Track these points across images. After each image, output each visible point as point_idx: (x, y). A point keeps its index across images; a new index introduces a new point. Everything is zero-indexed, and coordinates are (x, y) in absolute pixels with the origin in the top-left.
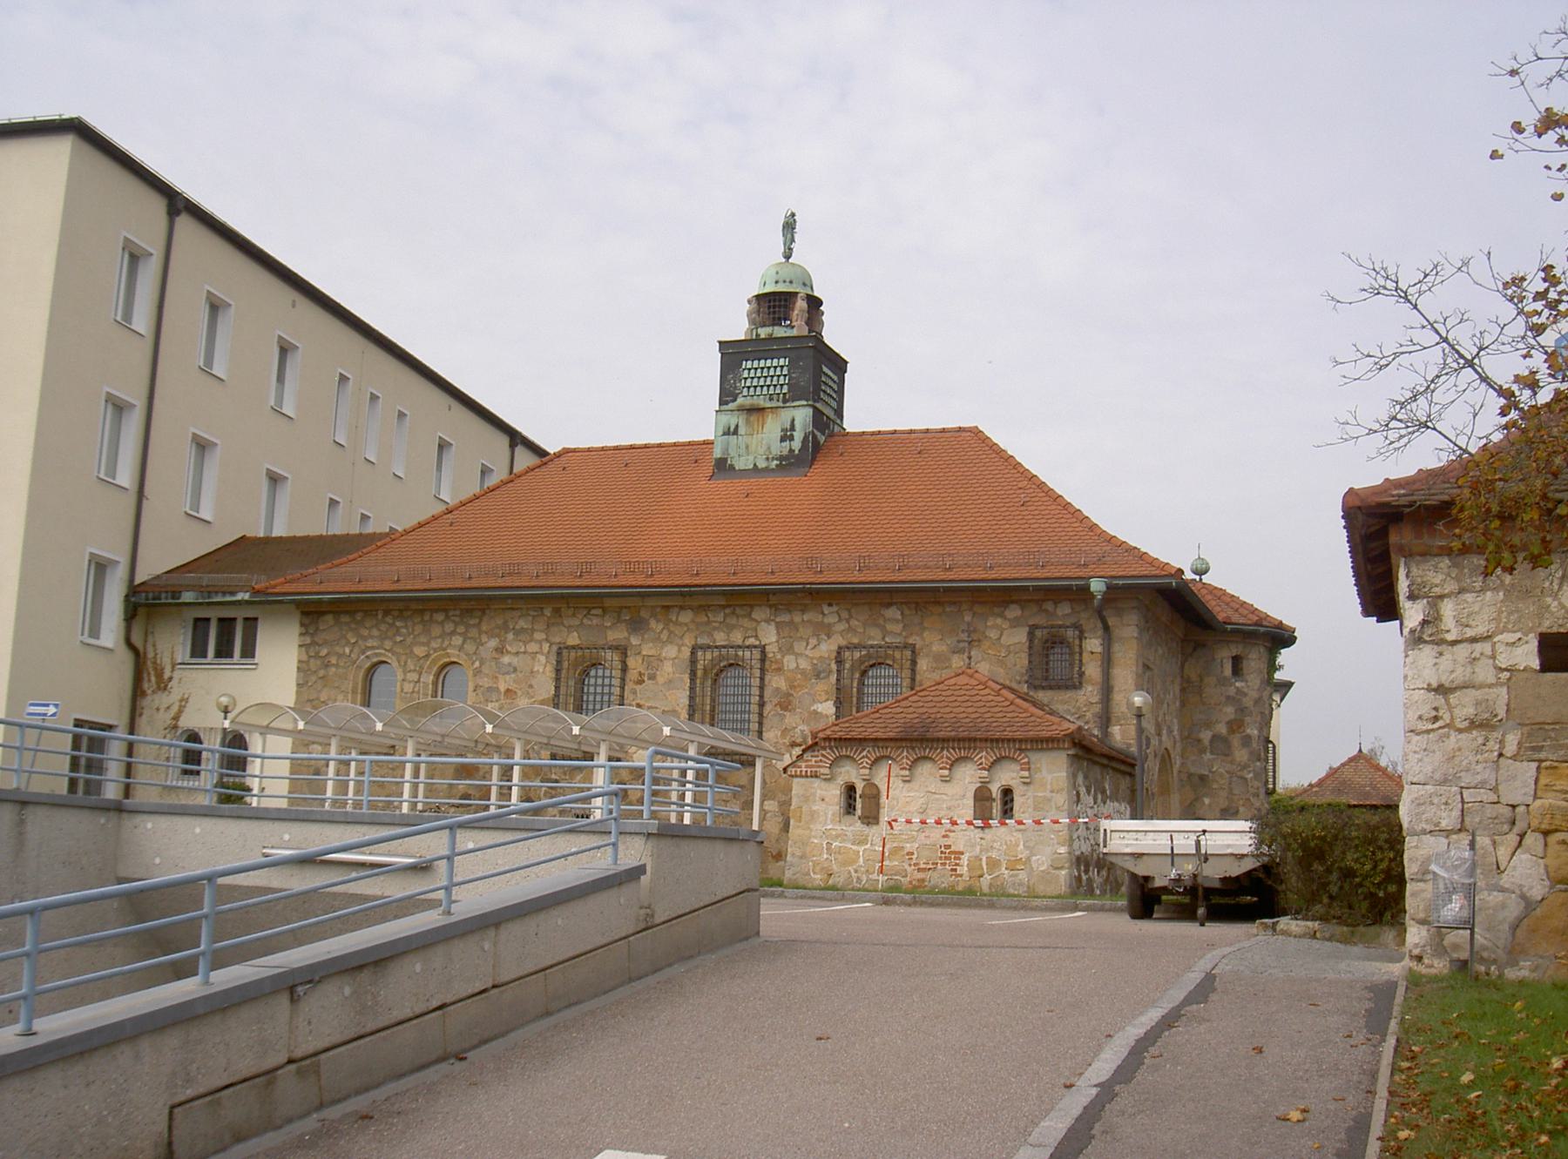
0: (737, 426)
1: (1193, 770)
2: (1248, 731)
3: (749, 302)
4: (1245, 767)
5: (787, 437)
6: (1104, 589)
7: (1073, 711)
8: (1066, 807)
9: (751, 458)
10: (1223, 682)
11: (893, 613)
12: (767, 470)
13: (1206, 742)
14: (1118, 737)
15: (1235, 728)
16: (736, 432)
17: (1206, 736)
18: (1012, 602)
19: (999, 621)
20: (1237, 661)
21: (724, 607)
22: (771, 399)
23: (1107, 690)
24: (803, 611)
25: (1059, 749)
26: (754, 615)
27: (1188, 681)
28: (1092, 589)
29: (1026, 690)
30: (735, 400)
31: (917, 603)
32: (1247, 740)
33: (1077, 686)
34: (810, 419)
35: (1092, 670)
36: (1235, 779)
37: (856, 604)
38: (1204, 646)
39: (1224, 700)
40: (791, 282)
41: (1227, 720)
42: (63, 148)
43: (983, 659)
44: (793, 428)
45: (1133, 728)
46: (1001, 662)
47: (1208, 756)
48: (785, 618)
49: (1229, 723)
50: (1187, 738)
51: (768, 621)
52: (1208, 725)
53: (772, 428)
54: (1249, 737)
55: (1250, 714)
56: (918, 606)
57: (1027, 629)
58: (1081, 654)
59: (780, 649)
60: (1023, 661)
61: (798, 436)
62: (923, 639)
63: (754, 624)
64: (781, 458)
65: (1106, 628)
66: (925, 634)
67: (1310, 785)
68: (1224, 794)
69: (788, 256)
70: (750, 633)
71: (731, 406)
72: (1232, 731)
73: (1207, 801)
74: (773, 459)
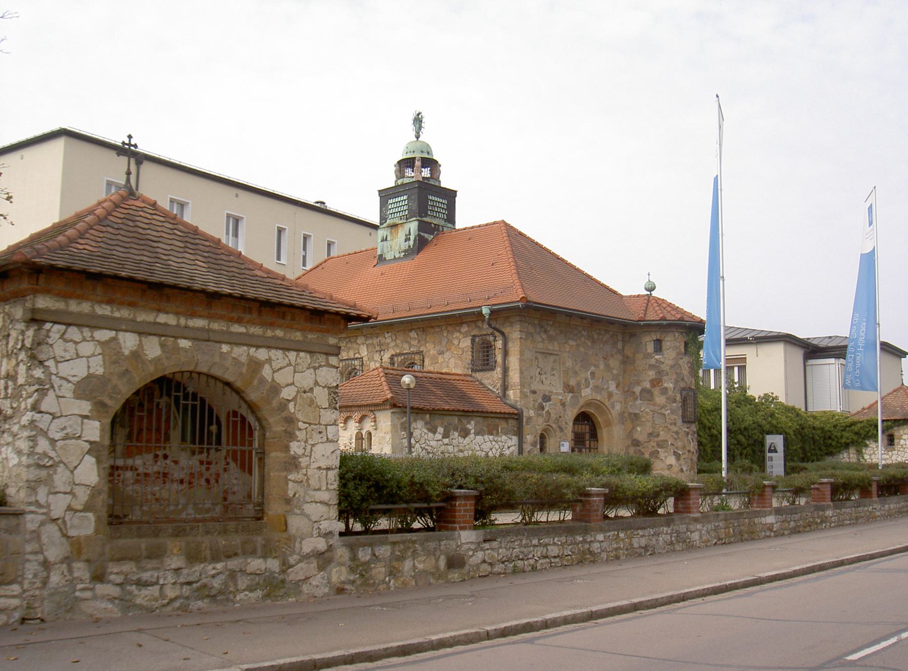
0: (387, 236)
1: (631, 411)
2: (665, 385)
3: (395, 166)
4: (663, 407)
5: (407, 239)
6: (489, 312)
7: (492, 383)
8: (390, 442)
9: (393, 252)
10: (648, 356)
11: (413, 334)
12: (399, 258)
13: (638, 393)
14: (512, 397)
15: (655, 383)
16: (386, 240)
17: (637, 390)
18: (463, 323)
19: (458, 334)
21: (346, 338)
22: (401, 219)
23: (505, 370)
24: (377, 337)
25: (384, 409)
26: (358, 341)
27: (627, 357)
28: (483, 313)
29: (470, 373)
30: (386, 222)
31: (423, 328)
32: (664, 391)
33: (493, 369)
34: (417, 228)
35: (499, 359)
36: (656, 415)
37: (398, 331)
38: (635, 335)
39: (647, 367)
40: (414, 152)
41: (650, 378)
42: (60, 144)
43: (452, 357)
44: (410, 234)
45: (518, 391)
46: (460, 358)
47: (639, 402)
48: (369, 342)
49: (652, 381)
50: (627, 391)
51: (363, 344)
52: (638, 383)
53: (401, 234)
54: (666, 389)
55: (667, 374)
56: (424, 330)
57: (471, 338)
58: (495, 349)
59: (368, 358)
60: (468, 356)
61: (412, 237)
62: (426, 348)
63: (358, 346)
64: (405, 251)
65: (503, 334)
66: (428, 344)
67: (864, 409)
68: (649, 424)
69: (418, 137)
70: (357, 351)
71: (385, 225)
72: (653, 386)
73: (639, 429)
74: (402, 252)
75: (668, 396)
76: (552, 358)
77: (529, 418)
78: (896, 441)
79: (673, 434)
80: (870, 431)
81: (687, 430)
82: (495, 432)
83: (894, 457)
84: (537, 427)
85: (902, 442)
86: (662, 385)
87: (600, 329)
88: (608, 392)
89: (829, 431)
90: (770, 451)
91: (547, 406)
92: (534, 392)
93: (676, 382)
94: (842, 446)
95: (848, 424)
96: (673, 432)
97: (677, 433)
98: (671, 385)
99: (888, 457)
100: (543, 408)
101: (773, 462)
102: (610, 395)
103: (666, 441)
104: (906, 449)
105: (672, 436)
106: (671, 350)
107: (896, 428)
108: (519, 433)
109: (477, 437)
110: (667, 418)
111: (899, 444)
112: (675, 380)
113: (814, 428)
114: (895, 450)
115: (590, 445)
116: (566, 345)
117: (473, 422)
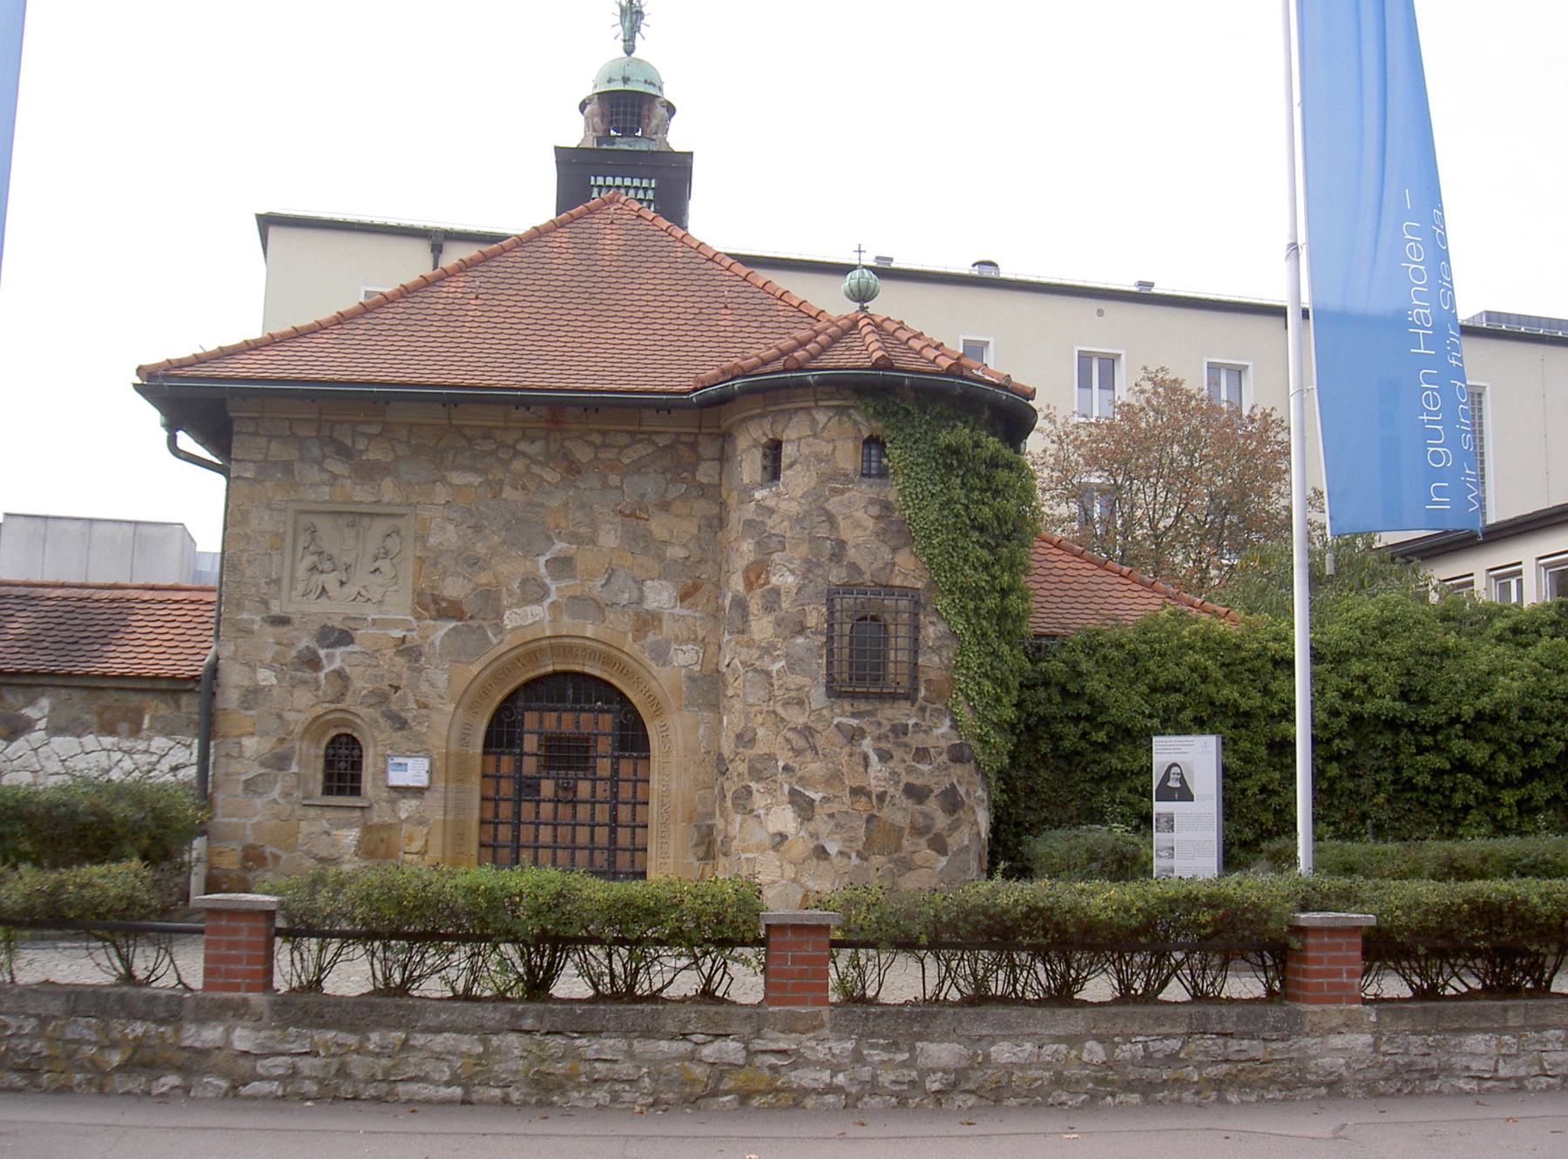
4: (768, 650)
20: (774, 449)
54: (776, 591)
75: (782, 614)
76: (381, 527)
77: (253, 695)
79: (790, 735)
81: (854, 722)
82: (124, 727)
84: (290, 716)
86: (767, 582)
87: (604, 433)
88: (637, 614)
90: (1167, 794)
91: (334, 659)
92: (282, 621)
93: (810, 566)
96: (790, 729)
97: (807, 732)
98: (790, 579)
100: (313, 663)
101: (1176, 835)
102: (647, 622)
103: (771, 757)
105: (788, 741)
106: (798, 467)
108: (208, 728)
109: (53, 739)
110: (775, 682)
112: (806, 561)
115: (615, 771)
116: (439, 487)
117: (45, 703)
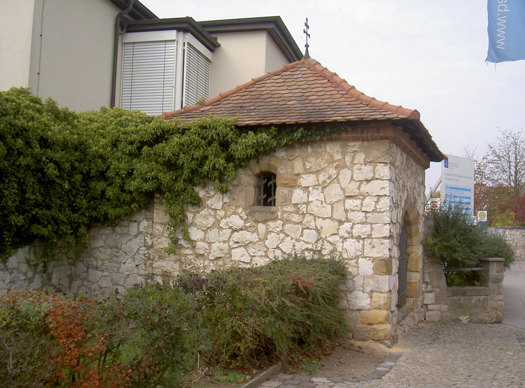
78: (280, 192)
80: (206, 158)
83: (272, 240)
85: (298, 195)
89: (101, 157)
94: (133, 200)
95: (146, 138)
99: (254, 237)
104: (308, 218)
107: (281, 154)
111: (287, 200)
113: (44, 142)
114: (275, 219)
